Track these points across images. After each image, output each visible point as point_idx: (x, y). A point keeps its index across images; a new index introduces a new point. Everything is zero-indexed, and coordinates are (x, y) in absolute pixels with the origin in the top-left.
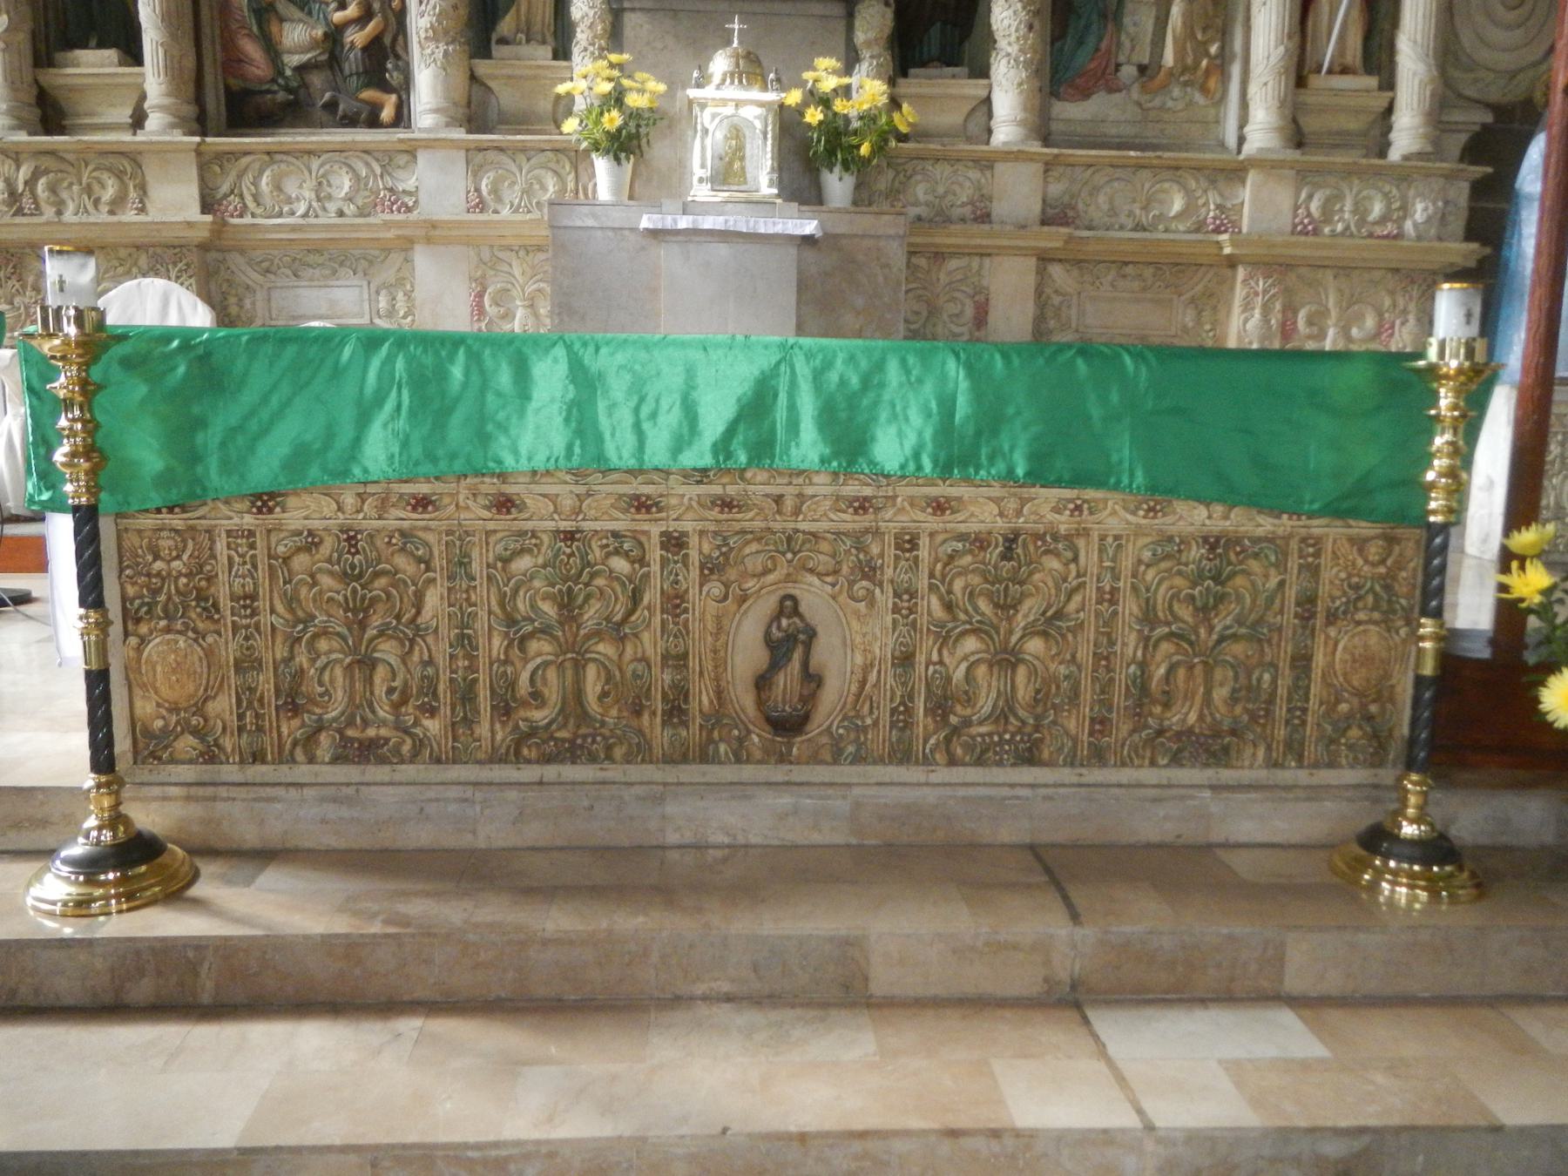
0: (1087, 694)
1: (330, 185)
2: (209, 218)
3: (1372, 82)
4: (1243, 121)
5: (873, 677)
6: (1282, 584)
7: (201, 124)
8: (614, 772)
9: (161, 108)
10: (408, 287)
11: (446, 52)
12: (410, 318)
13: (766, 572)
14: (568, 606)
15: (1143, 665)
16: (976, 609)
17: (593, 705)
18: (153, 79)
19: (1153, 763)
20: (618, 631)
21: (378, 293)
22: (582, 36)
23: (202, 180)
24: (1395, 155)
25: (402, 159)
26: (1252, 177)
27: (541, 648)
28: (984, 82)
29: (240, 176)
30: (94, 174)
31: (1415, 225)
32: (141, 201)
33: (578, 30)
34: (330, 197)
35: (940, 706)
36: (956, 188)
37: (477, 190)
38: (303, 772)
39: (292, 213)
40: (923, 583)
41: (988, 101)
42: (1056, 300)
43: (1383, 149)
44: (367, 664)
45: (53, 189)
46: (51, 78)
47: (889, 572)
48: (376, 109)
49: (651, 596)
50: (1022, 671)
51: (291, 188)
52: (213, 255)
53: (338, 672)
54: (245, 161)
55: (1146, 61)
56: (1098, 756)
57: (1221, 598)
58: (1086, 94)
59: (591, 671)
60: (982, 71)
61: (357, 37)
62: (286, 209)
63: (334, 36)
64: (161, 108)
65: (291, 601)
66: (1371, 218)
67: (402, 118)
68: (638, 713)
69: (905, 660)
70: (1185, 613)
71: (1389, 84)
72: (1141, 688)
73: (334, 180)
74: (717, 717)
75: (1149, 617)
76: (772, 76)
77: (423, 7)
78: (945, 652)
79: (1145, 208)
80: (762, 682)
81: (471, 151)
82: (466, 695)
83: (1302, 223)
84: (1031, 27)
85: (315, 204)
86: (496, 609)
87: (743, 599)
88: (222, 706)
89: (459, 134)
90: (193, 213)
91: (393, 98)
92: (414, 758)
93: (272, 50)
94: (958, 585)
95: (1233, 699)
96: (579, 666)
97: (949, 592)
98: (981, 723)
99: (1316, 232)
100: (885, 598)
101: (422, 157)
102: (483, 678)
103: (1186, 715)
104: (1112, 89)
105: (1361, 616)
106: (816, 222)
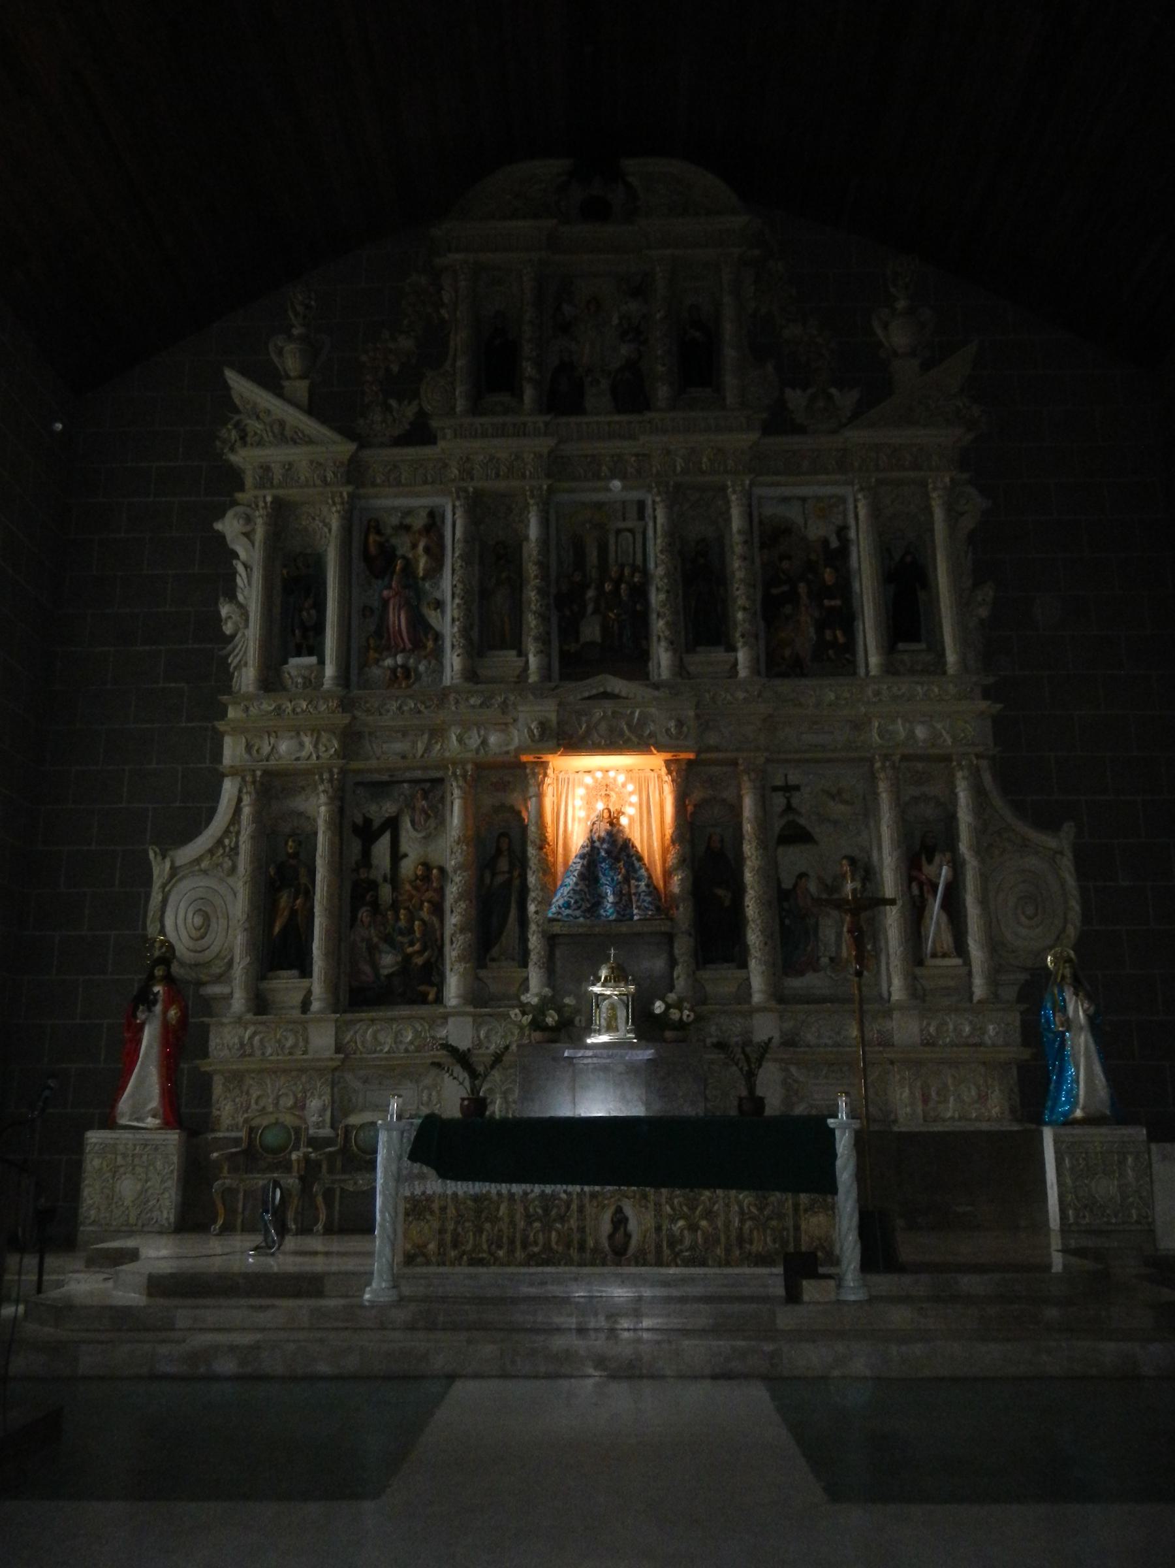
0: (723, 1240)
1: (402, 1035)
2: (342, 1056)
3: (958, 961)
4: (890, 984)
5: (648, 1234)
6: (787, 1199)
7: (336, 1006)
8: (561, 1269)
9: (319, 999)
10: (439, 1088)
11: (465, 968)
12: (438, 1106)
13: (611, 1197)
14: (546, 1211)
15: (741, 1229)
16: (682, 1210)
17: (554, 1246)
18: (317, 985)
19: (749, 1267)
20: (562, 1219)
21: (422, 1092)
22: (534, 957)
23: (336, 1033)
24: (976, 998)
25: (439, 1021)
26: (896, 1015)
27: (537, 1225)
28: (746, 970)
29: (356, 1033)
30: (285, 1033)
31: (990, 1038)
32: (306, 1047)
33: (532, 954)
34: (401, 1042)
35: (672, 1244)
36: (734, 1029)
37: (478, 1037)
38: (458, 1269)
39: (381, 1050)
40: (663, 1200)
41: (748, 979)
42: (796, 1086)
43: (971, 999)
44: (479, 1230)
45: (261, 1041)
46: (265, 985)
47: (652, 1197)
48: (426, 995)
49: (574, 1207)
50: (699, 1233)
51: (381, 1037)
52: (337, 1074)
53: (471, 1234)
54: (358, 1027)
55: (833, 955)
56: (728, 1264)
57: (767, 1204)
58: (802, 973)
59: (554, 1234)
60: (744, 965)
61: (419, 961)
62: (378, 1049)
63: (407, 958)
64: (319, 999)
65: (457, 1210)
66: (964, 1034)
67: (439, 1000)
68: (569, 1249)
69: (658, 1229)
70: (753, 1210)
71: (967, 962)
72: (741, 1240)
73: (405, 1033)
74: (596, 1250)
75: (742, 1212)
76: (630, 978)
77: (454, 945)
78: (673, 1225)
79: (839, 1033)
80: (611, 1237)
81: (474, 1016)
82: (512, 1242)
83: (926, 1039)
84: (766, 944)
85: (393, 1046)
86: (522, 1211)
87: (603, 1207)
88: (432, 1246)
89: (470, 1009)
90: (331, 1053)
91: (435, 989)
92: (494, 1264)
93: (375, 966)
94: (676, 1201)
95: (774, 1241)
96: (550, 1232)
97: (673, 1203)
98: (687, 1251)
99: (934, 1045)
100: (651, 1206)
101: (451, 1020)
102: (518, 1235)
103: (756, 1247)
104: (815, 970)
105: (816, 1210)
106: (653, 1051)
